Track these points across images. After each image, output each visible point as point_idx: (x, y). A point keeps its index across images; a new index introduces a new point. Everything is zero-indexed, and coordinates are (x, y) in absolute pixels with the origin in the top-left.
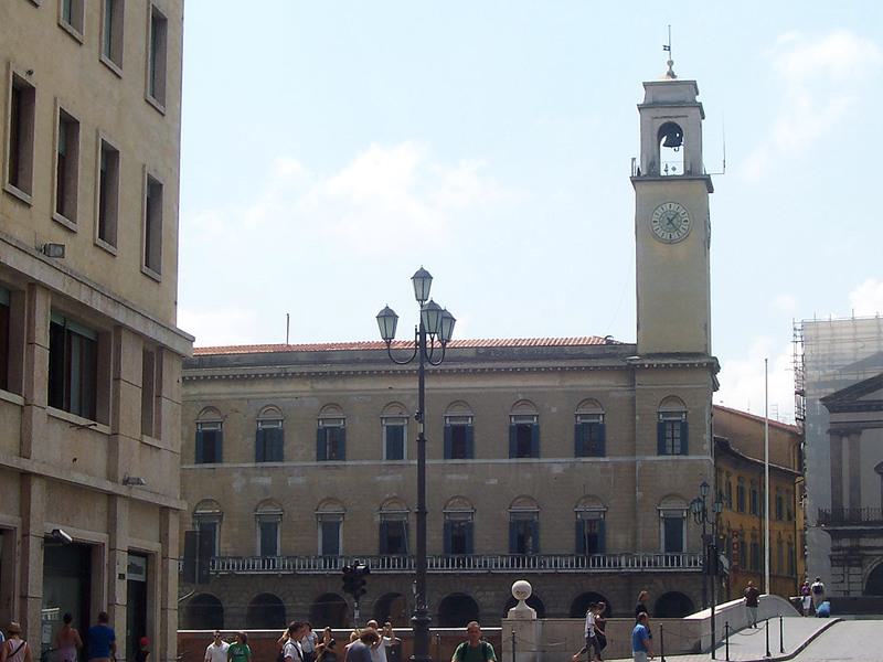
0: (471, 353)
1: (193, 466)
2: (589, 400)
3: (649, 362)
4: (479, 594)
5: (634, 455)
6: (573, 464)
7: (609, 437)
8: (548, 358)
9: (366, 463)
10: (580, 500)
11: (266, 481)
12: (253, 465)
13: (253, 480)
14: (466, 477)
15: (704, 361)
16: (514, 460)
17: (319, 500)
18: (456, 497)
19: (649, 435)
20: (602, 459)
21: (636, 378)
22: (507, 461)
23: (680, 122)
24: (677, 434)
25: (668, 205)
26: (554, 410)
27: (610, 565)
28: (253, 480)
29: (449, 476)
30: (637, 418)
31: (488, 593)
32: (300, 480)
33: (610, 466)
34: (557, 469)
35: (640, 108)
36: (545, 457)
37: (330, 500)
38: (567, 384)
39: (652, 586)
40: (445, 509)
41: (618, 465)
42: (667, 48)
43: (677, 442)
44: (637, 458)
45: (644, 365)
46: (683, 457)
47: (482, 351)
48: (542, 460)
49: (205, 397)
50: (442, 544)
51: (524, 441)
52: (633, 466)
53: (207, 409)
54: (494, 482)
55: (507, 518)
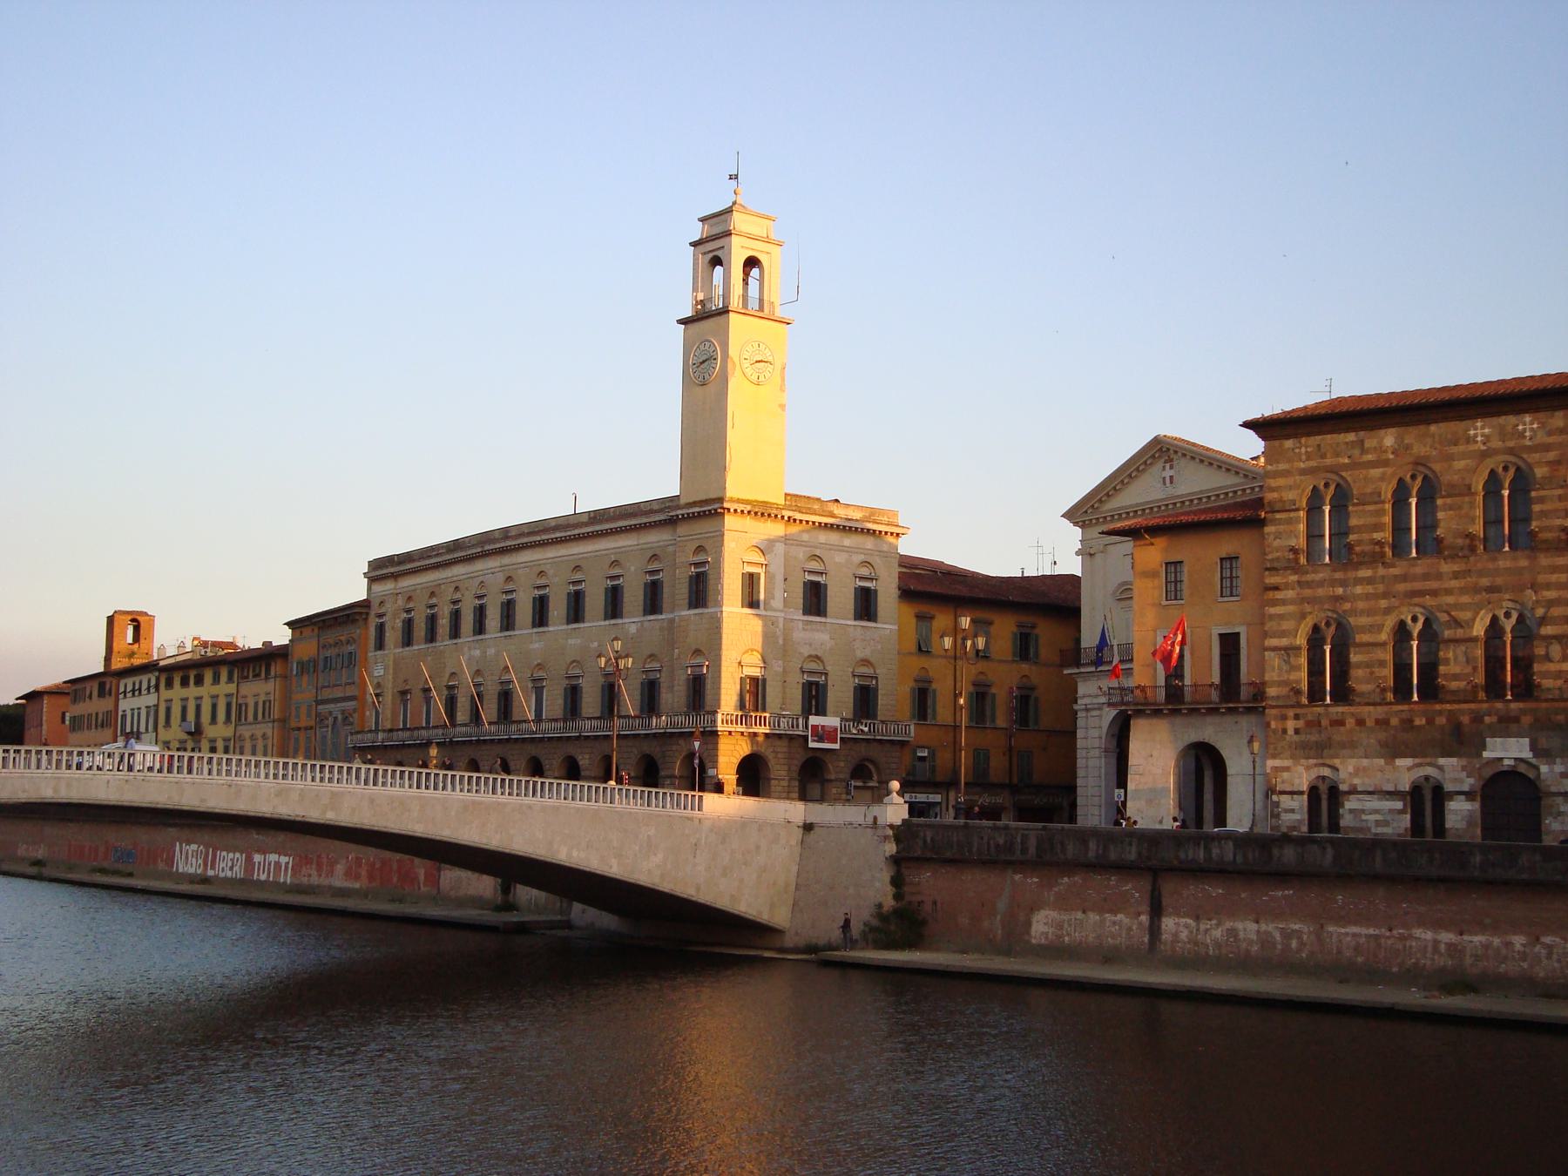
0: (585, 519)
1: (448, 643)
8: (608, 520)
10: (646, 660)
18: (574, 661)
22: (603, 623)
29: (570, 641)
35: (695, 244)
42: (732, 177)
45: (677, 516)
47: (592, 515)
51: (614, 604)
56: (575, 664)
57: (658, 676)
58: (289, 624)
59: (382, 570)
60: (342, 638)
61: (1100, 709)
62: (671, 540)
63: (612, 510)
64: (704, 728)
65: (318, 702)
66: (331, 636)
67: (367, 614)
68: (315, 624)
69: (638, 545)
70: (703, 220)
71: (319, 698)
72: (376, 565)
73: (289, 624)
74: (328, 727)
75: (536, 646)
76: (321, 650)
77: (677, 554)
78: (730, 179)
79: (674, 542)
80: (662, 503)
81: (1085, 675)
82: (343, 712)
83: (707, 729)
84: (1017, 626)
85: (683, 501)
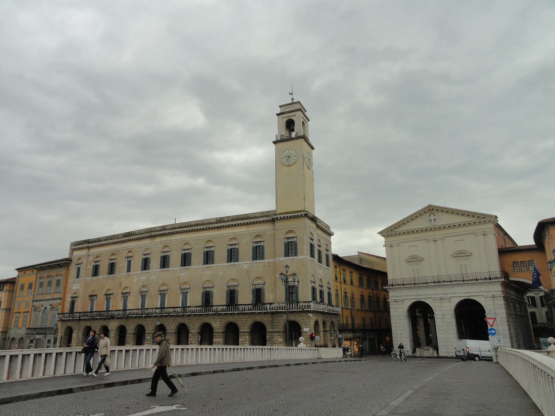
0: (215, 221)
2: (258, 236)
3: (280, 216)
4: (214, 323)
5: (275, 257)
6: (252, 264)
7: (266, 250)
9: (176, 268)
11: (144, 278)
12: (141, 272)
13: (140, 278)
14: (211, 272)
15: (303, 213)
16: (229, 264)
17: (160, 284)
18: (208, 281)
19: (281, 249)
20: (263, 261)
21: (275, 223)
22: (226, 264)
23: (293, 118)
24: (293, 247)
25: (288, 151)
26: (245, 241)
27: (264, 309)
28: (140, 278)
29: (205, 272)
30: (276, 241)
31: (217, 323)
32: (154, 277)
33: (266, 264)
34: (245, 266)
35: (278, 115)
36: (242, 261)
37: (163, 284)
38: (250, 229)
39: (282, 318)
40: (203, 286)
41: (269, 263)
43: (293, 251)
44: (276, 259)
46: (295, 257)
47: (218, 219)
48: (240, 263)
49: (129, 248)
50: (201, 301)
52: (275, 263)
53: (130, 252)
54: (221, 273)
55: (226, 289)
56: (208, 282)
57: (263, 286)
58: (17, 269)
59: (77, 246)
60: (53, 274)
61: (403, 301)
62: (273, 228)
63: (231, 217)
64: (303, 309)
65: (33, 301)
66: (45, 274)
67: (70, 264)
68: (36, 269)
69: (247, 231)
70: (280, 107)
71: (35, 299)
72: (72, 244)
73: (17, 269)
74: (40, 311)
75: (183, 274)
76: (38, 279)
77: (276, 234)
78: (290, 94)
79: (274, 229)
80: (263, 214)
81: (395, 289)
82: (51, 305)
83: (304, 310)
84: (350, 272)
85: (278, 212)
